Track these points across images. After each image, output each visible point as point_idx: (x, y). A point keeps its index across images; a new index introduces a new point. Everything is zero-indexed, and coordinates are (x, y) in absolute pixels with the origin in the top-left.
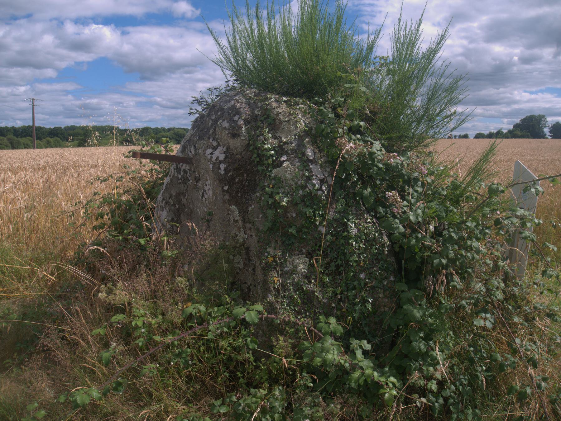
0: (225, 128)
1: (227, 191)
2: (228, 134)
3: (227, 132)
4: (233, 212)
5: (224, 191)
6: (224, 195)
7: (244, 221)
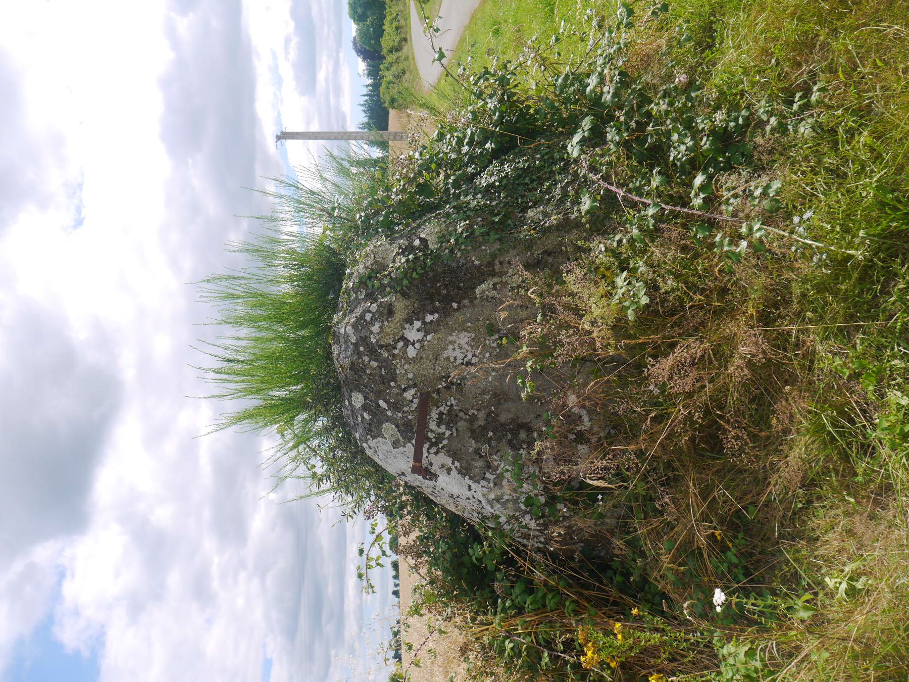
0: (381, 328)
1: (459, 303)
2: (388, 322)
3: (386, 323)
4: (483, 292)
5: (459, 308)
6: (464, 306)
7: (493, 274)
